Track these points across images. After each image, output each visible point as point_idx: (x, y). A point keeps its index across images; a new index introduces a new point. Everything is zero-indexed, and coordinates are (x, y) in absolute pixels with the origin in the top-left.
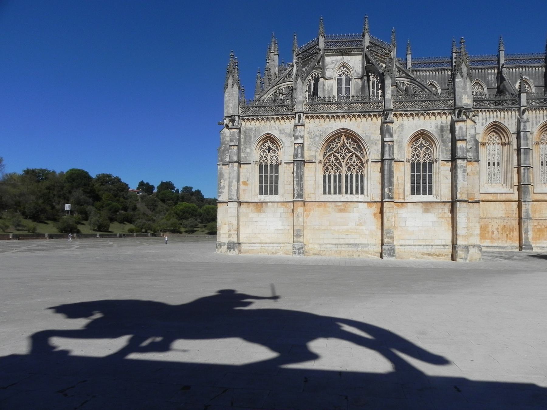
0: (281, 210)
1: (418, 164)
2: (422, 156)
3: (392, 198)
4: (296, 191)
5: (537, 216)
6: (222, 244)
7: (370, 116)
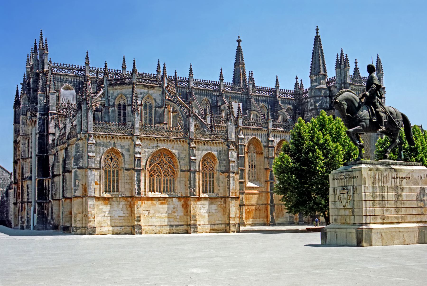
0: (122, 203)
2: (208, 169)
3: (195, 196)
4: (136, 190)
5: (247, 203)
6: (78, 229)
7: (180, 141)
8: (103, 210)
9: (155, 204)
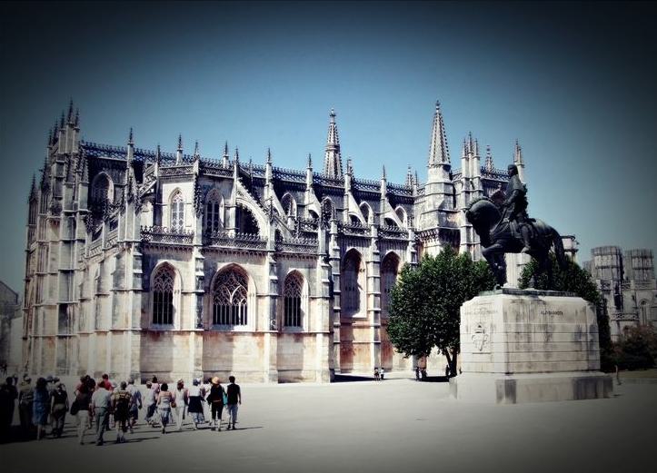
1: (291, 299)
7: (256, 254)
8: (151, 348)
9: (220, 342)
